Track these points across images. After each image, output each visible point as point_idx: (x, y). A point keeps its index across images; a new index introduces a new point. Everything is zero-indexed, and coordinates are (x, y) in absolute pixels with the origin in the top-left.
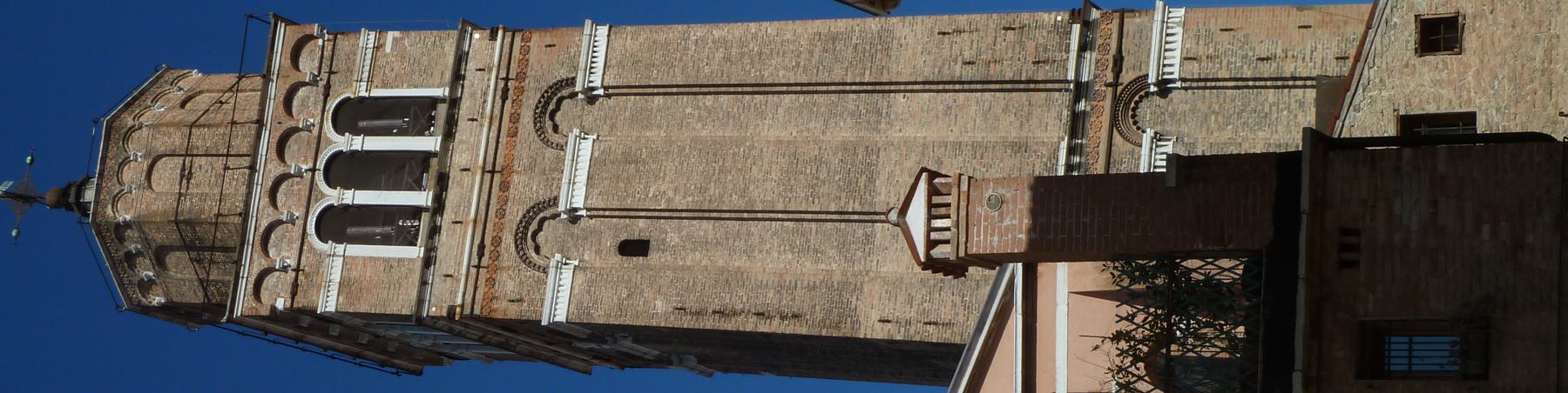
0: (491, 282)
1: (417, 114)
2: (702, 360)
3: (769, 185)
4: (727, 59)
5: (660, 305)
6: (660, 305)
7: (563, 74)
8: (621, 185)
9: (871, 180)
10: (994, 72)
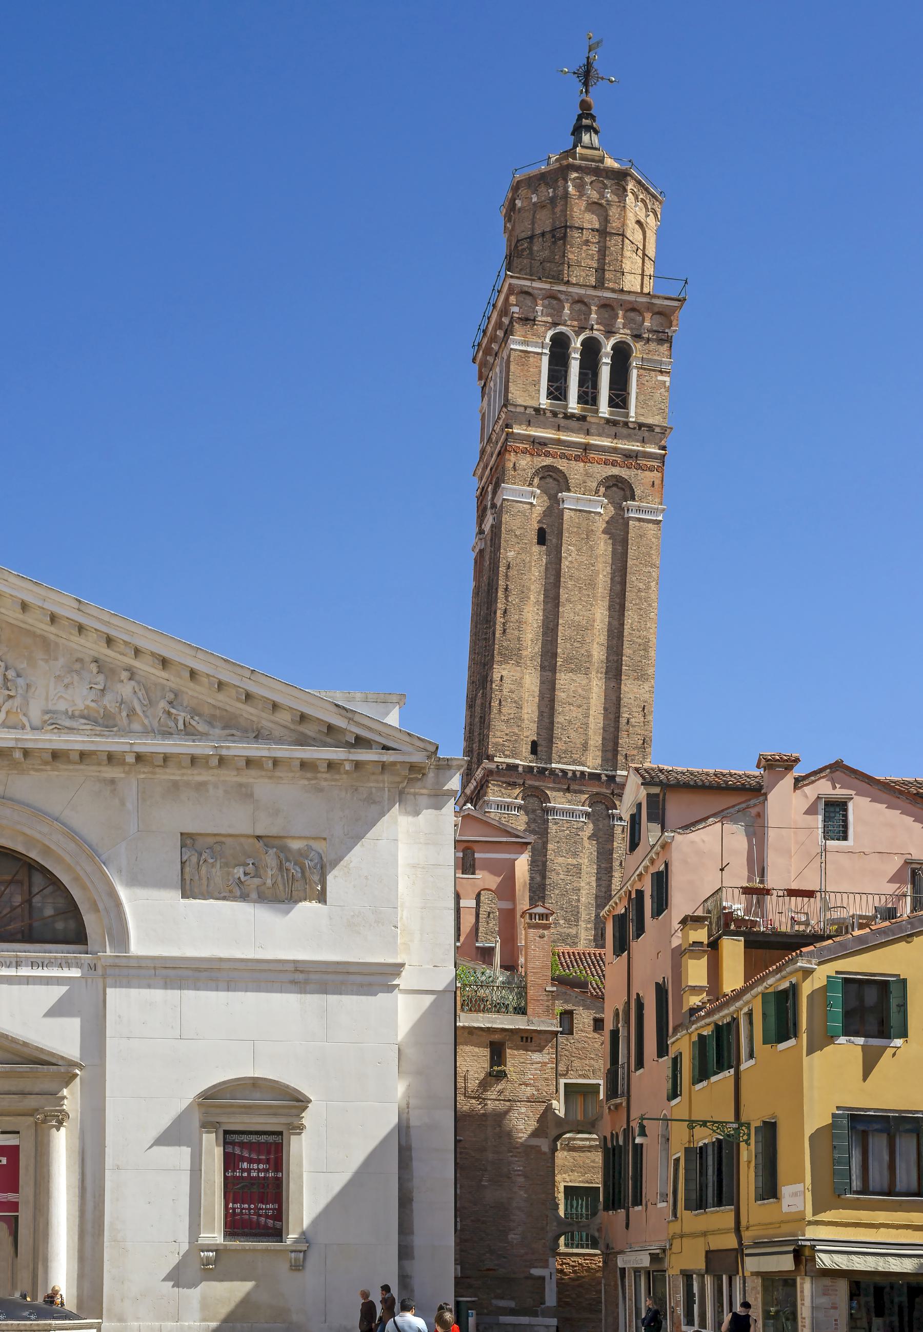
0: (525, 451)
1: (619, 400)
2: (481, 551)
3: (572, 615)
4: (639, 590)
5: (511, 554)
6: (511, 554)
7: (638, 492)
8: (575, 530)
9: (572, 671)
10: (623, 734)
